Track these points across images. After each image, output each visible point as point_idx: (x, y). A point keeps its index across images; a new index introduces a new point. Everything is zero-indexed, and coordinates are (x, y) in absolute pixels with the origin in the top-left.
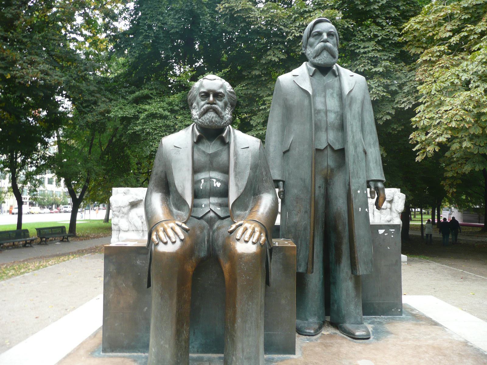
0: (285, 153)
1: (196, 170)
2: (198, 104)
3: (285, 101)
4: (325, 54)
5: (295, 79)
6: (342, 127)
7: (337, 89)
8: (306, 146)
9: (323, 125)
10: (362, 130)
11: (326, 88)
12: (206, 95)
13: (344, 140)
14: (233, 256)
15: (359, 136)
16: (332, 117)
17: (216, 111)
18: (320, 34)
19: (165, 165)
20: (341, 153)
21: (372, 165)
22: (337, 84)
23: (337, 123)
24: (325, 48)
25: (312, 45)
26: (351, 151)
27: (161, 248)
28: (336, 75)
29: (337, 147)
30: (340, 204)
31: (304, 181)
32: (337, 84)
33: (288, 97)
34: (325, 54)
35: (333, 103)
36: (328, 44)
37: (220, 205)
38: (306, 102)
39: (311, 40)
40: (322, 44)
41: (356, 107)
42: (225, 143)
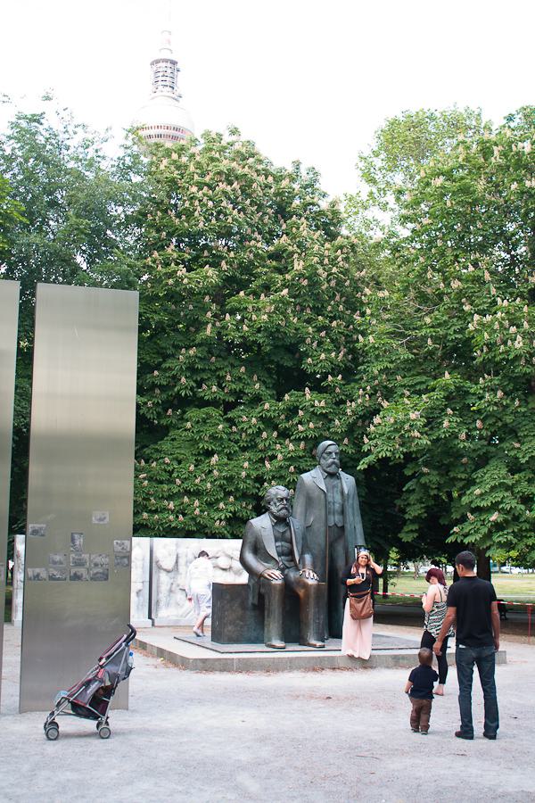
0: (307, 527)
1: (276, 541)
2: (275, 504)
3: (308, 494)
4: (334, 466)
5: (315, 480)
6: (343, 512)
7: (339, 488)
8: (322, 524)
9: (332, 510)
10: (353, 514)
11: (334, 487)
12: (282, 499)
13: (344, 520)
14: (305, 586)
15: (352, 518)
16: (337, 506)
17: (286, 509)
18: (330, 453)
19: (256, 538)
20: (343, 528)
21: (359, 536)
22: (339, 485)
23: (340, 510)
24: (333, 463)
25: (324, 459)
26: (348, 527)
27: (274, 582)
28: (339, 478)
29: (340, 525)
30: (341, 563)
31: (320, 545)
32: (339, 485)
33: (310, 492)
34: (334, 466)
35: (338, 498)
36: (336, 460)
37: (287, 561)
38: (323, 496)
39: (325, 455)
40: (331, 460)
41: (351, 496)
42: (288, 525)
